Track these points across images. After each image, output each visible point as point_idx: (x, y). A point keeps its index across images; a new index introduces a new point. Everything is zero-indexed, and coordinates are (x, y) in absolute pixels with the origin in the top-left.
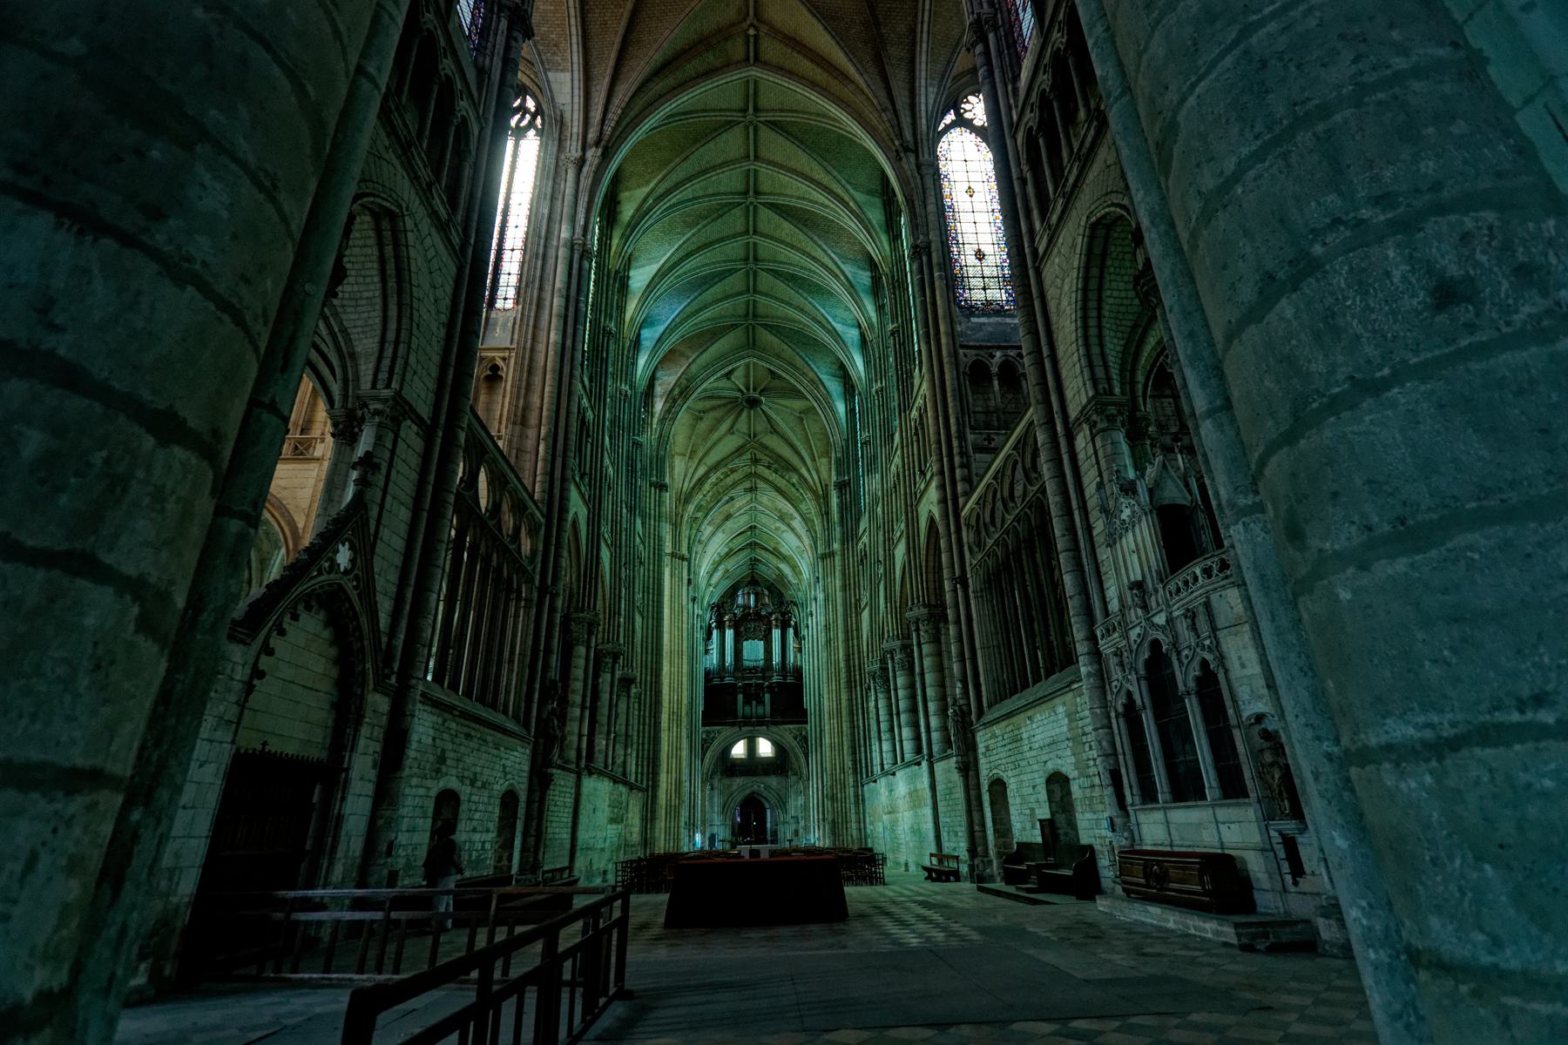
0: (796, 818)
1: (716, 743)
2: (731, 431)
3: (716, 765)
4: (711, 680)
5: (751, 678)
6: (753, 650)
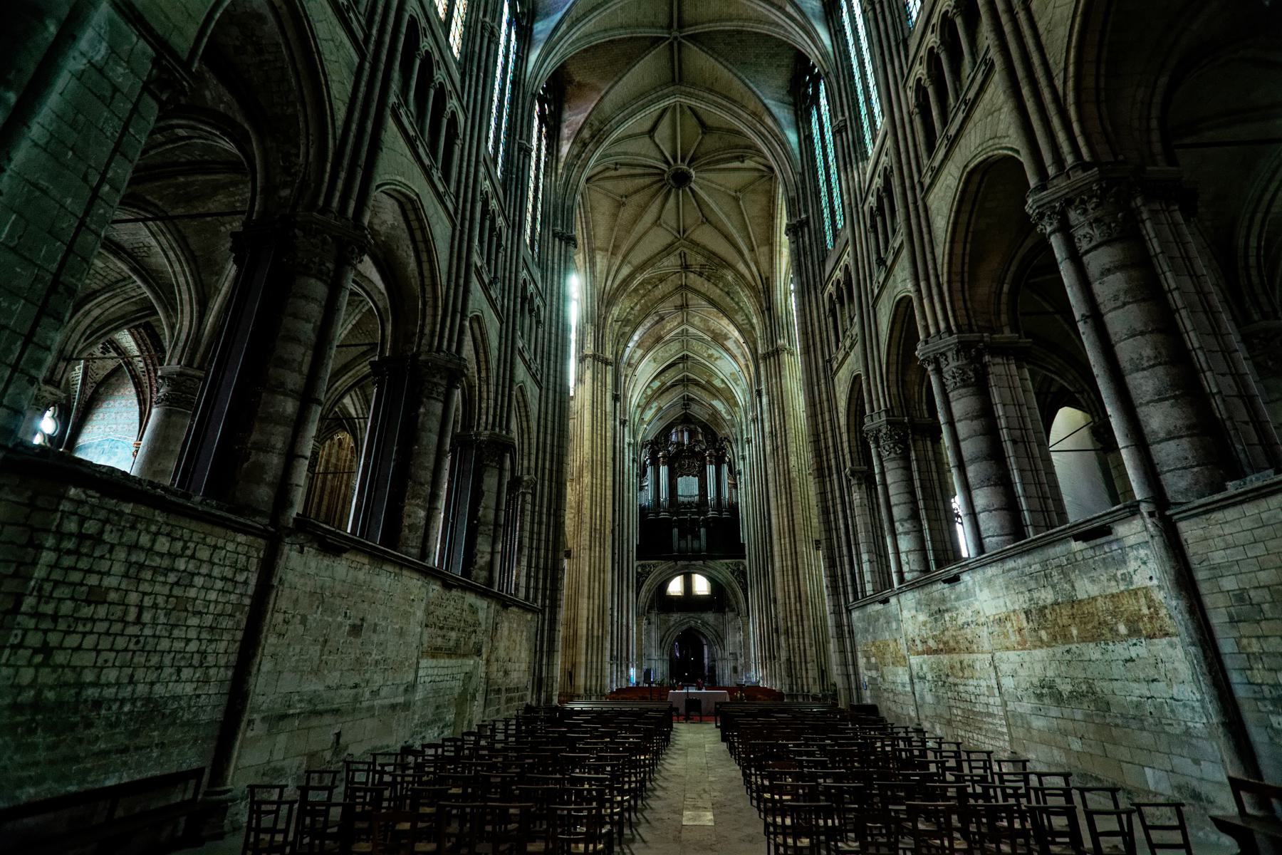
0: (734, 654)
1: (651, 577)
2: (657, 222)
3: (652, 600)
4: (647, 515)
5: (685, 514)
6: (688, 487)
